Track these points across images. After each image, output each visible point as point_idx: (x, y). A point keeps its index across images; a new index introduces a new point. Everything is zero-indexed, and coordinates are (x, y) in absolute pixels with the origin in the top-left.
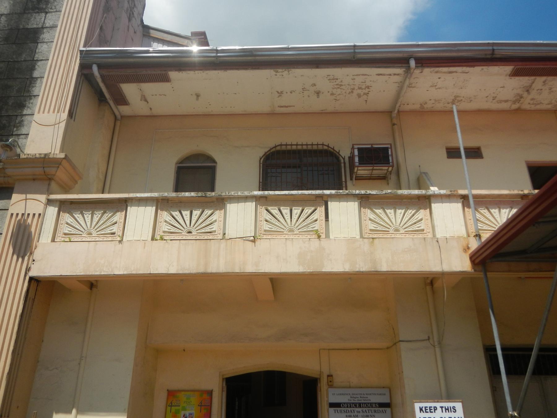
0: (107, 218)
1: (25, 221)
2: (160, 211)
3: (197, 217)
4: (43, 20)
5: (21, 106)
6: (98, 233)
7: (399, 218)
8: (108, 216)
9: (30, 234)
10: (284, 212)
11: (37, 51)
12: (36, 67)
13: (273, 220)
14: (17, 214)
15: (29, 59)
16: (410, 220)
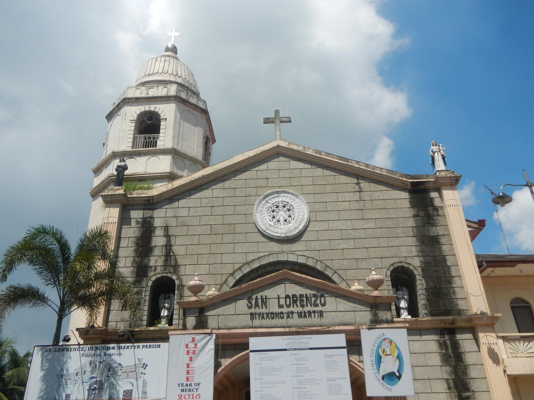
1: (490, 346)
4: (436, 231)
5: (450, 282)
6: (526, 352)
9: (496, 354)
11: (442, 250)
12: (447, 259)
14: (486, 344)
15: (440, 255)
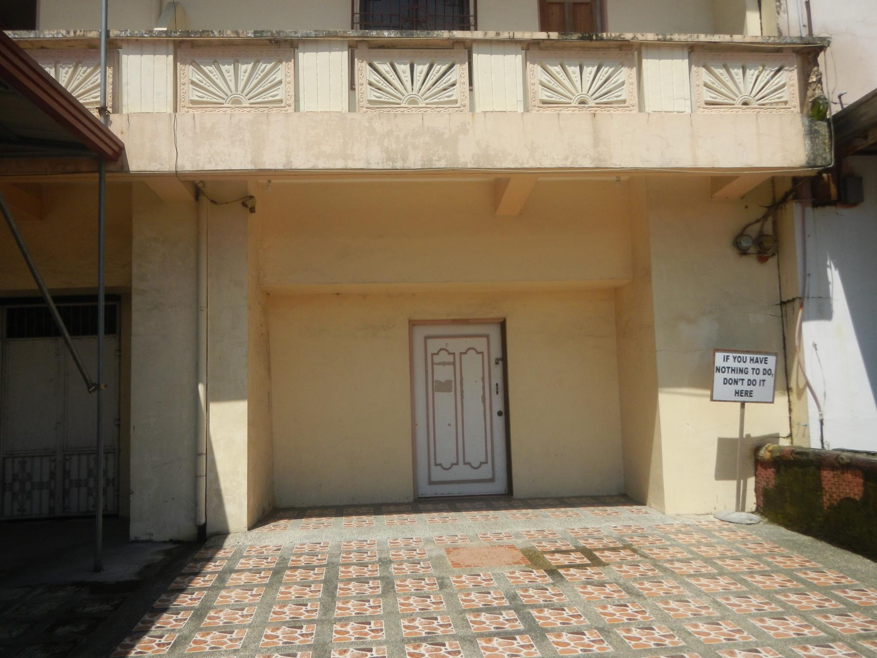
0: (86, 74)
2: (181, 64)
3: (247, 74)
7: (751, 82)
8: (85, 71)
10: (400, 68)
13: (382, 83)
16: (605, 85)
